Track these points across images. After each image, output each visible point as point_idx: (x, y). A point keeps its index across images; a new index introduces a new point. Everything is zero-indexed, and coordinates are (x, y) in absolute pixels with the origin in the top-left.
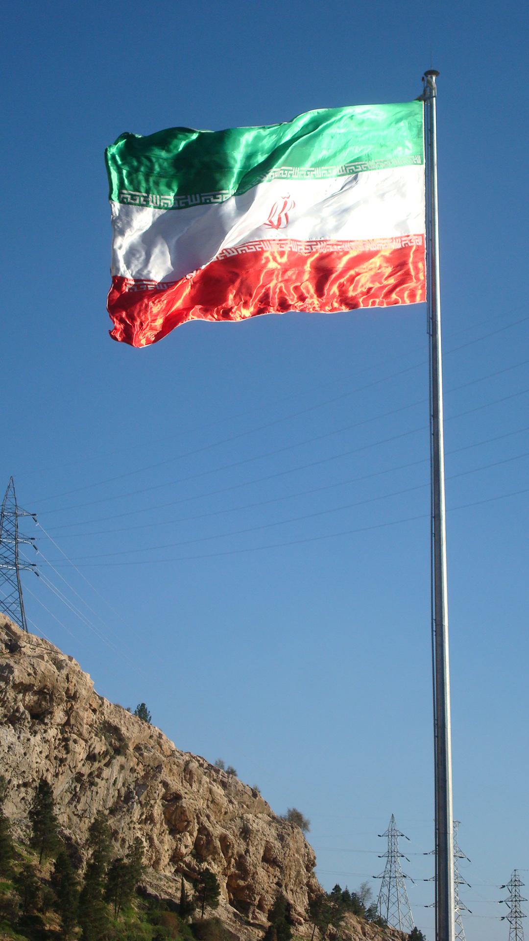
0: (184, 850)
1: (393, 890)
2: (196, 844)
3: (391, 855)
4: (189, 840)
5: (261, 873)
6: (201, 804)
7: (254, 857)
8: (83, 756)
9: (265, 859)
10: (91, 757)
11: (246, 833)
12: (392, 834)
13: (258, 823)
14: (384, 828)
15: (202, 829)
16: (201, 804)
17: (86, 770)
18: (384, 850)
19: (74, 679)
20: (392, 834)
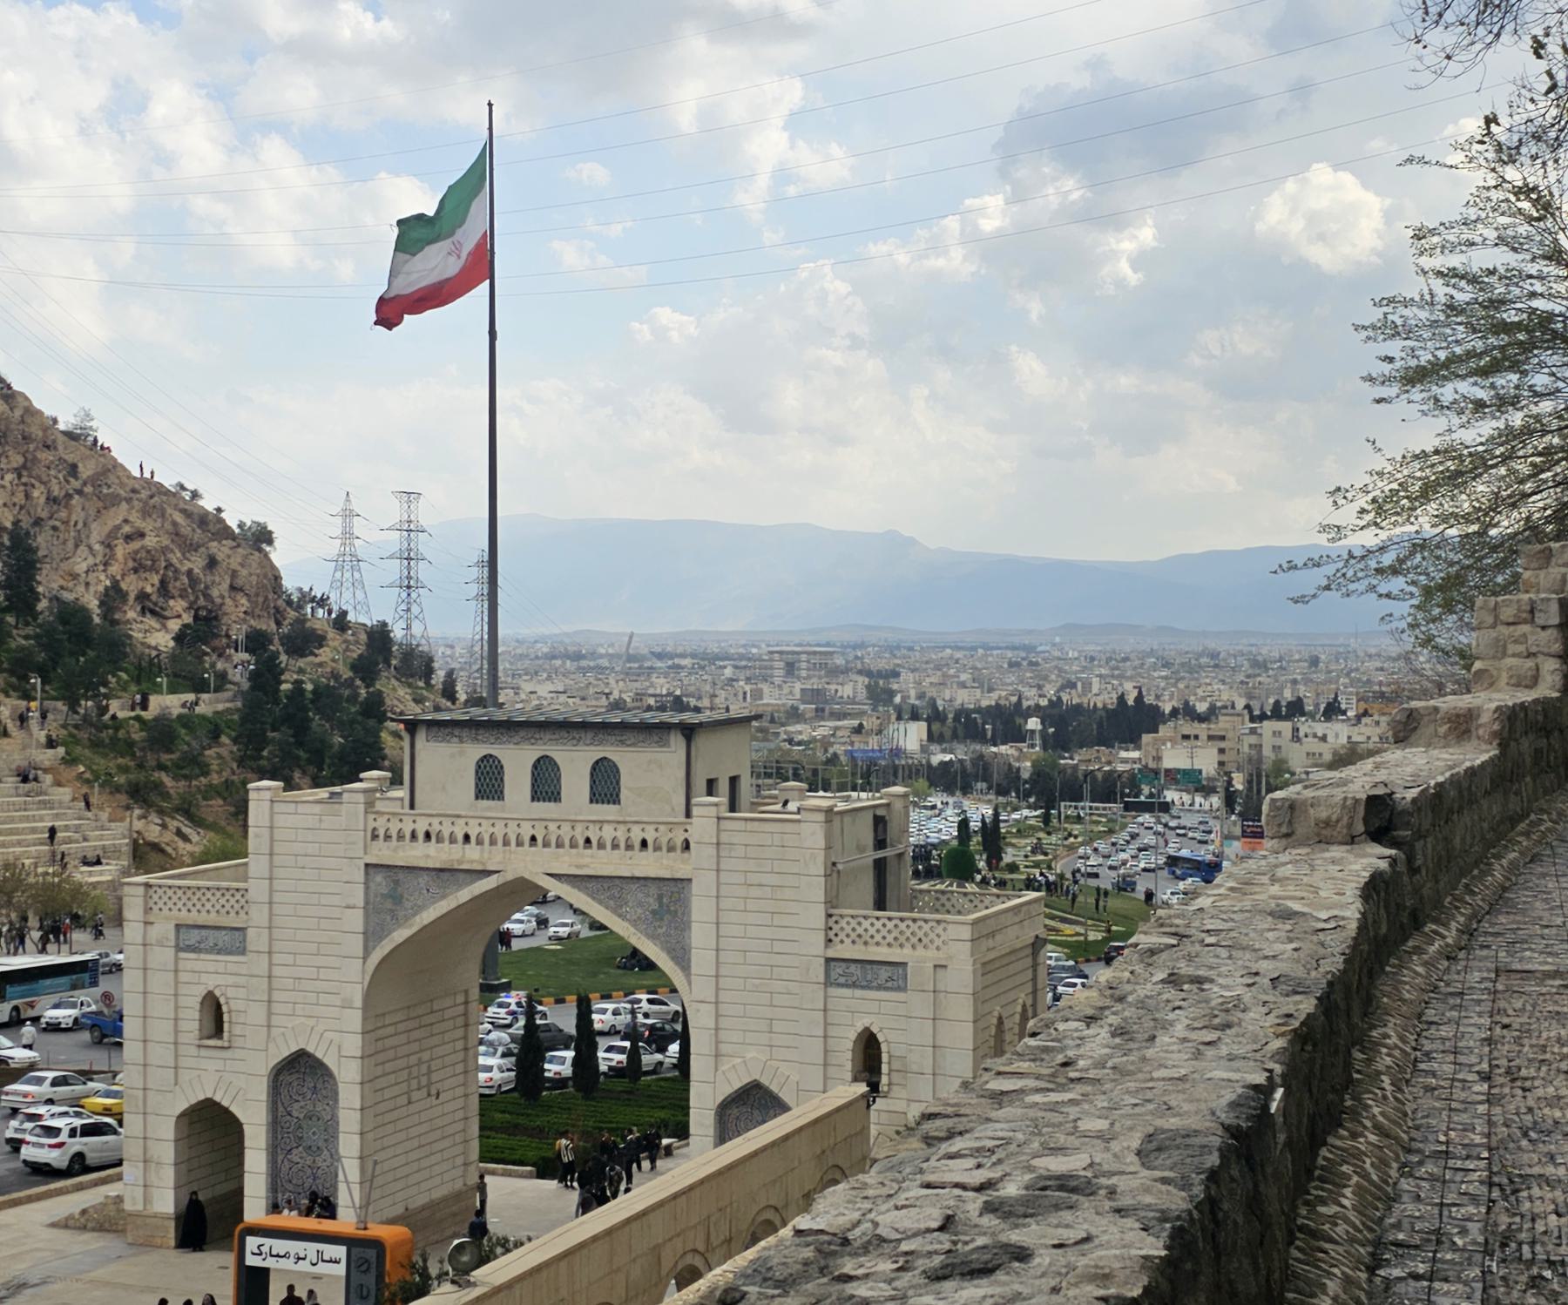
0: (149, 589)
1: (347, 575)
2: (163, 582)
3: (348, 536)
4: (156, 579)
5: (228, 601)
6: (166, 541)
7: (219, 590)
8: (43, 500)
9: (232, 588)
10: (52, 500)
11: (212, 563)
12: (348, 514)
13: (221, 550)
14: (337, 509)
15: (169, 565)
16: (166, 541)
17: (44, 515)
18: (338, 532)
19: (28, 420)
20: (348, 514)
